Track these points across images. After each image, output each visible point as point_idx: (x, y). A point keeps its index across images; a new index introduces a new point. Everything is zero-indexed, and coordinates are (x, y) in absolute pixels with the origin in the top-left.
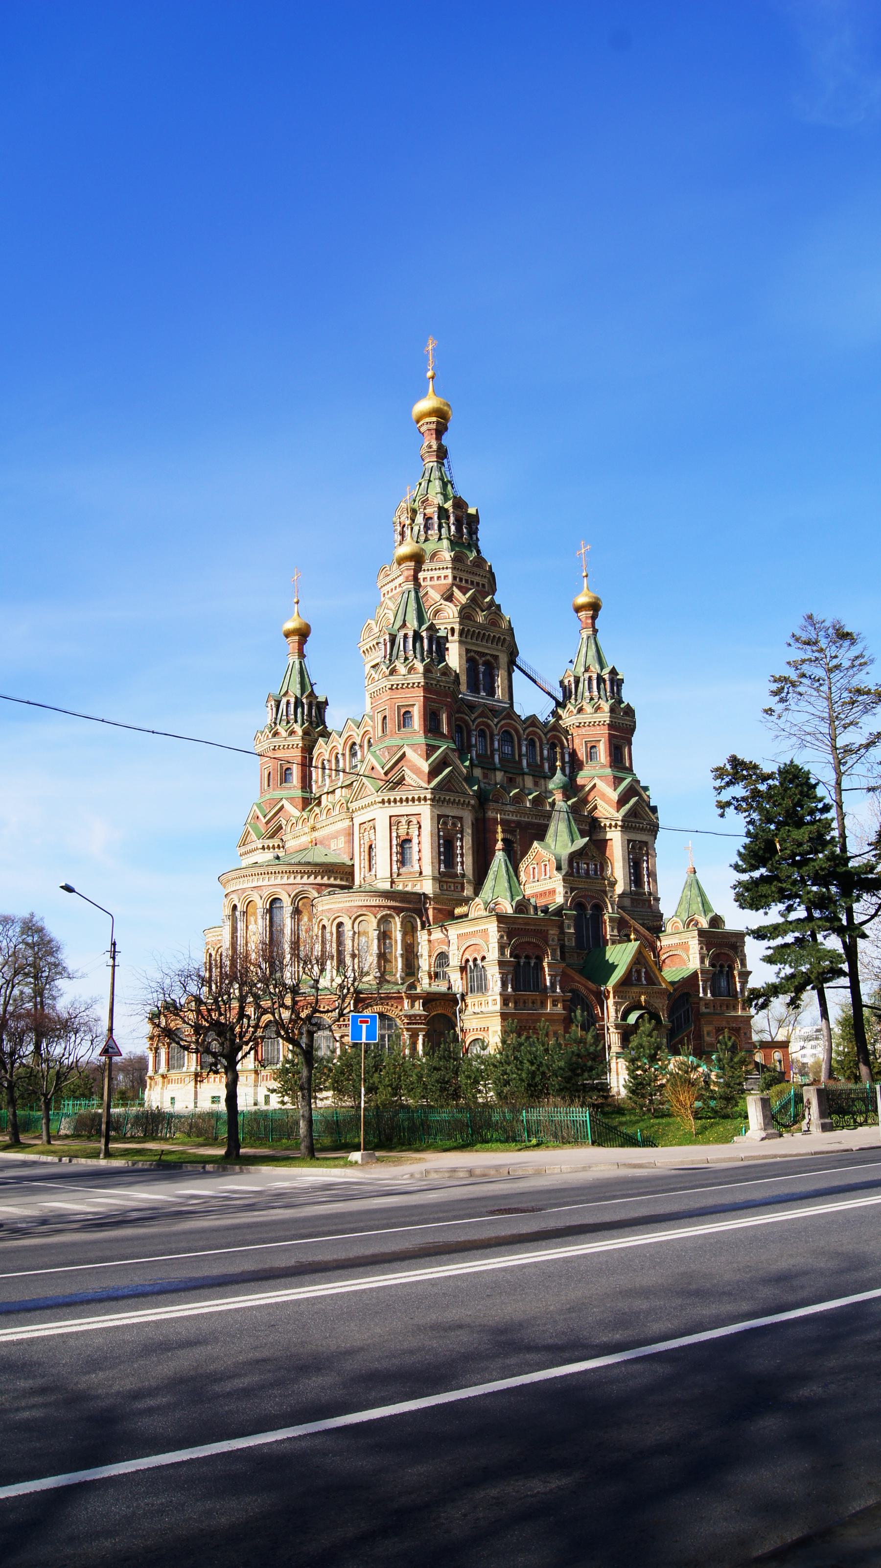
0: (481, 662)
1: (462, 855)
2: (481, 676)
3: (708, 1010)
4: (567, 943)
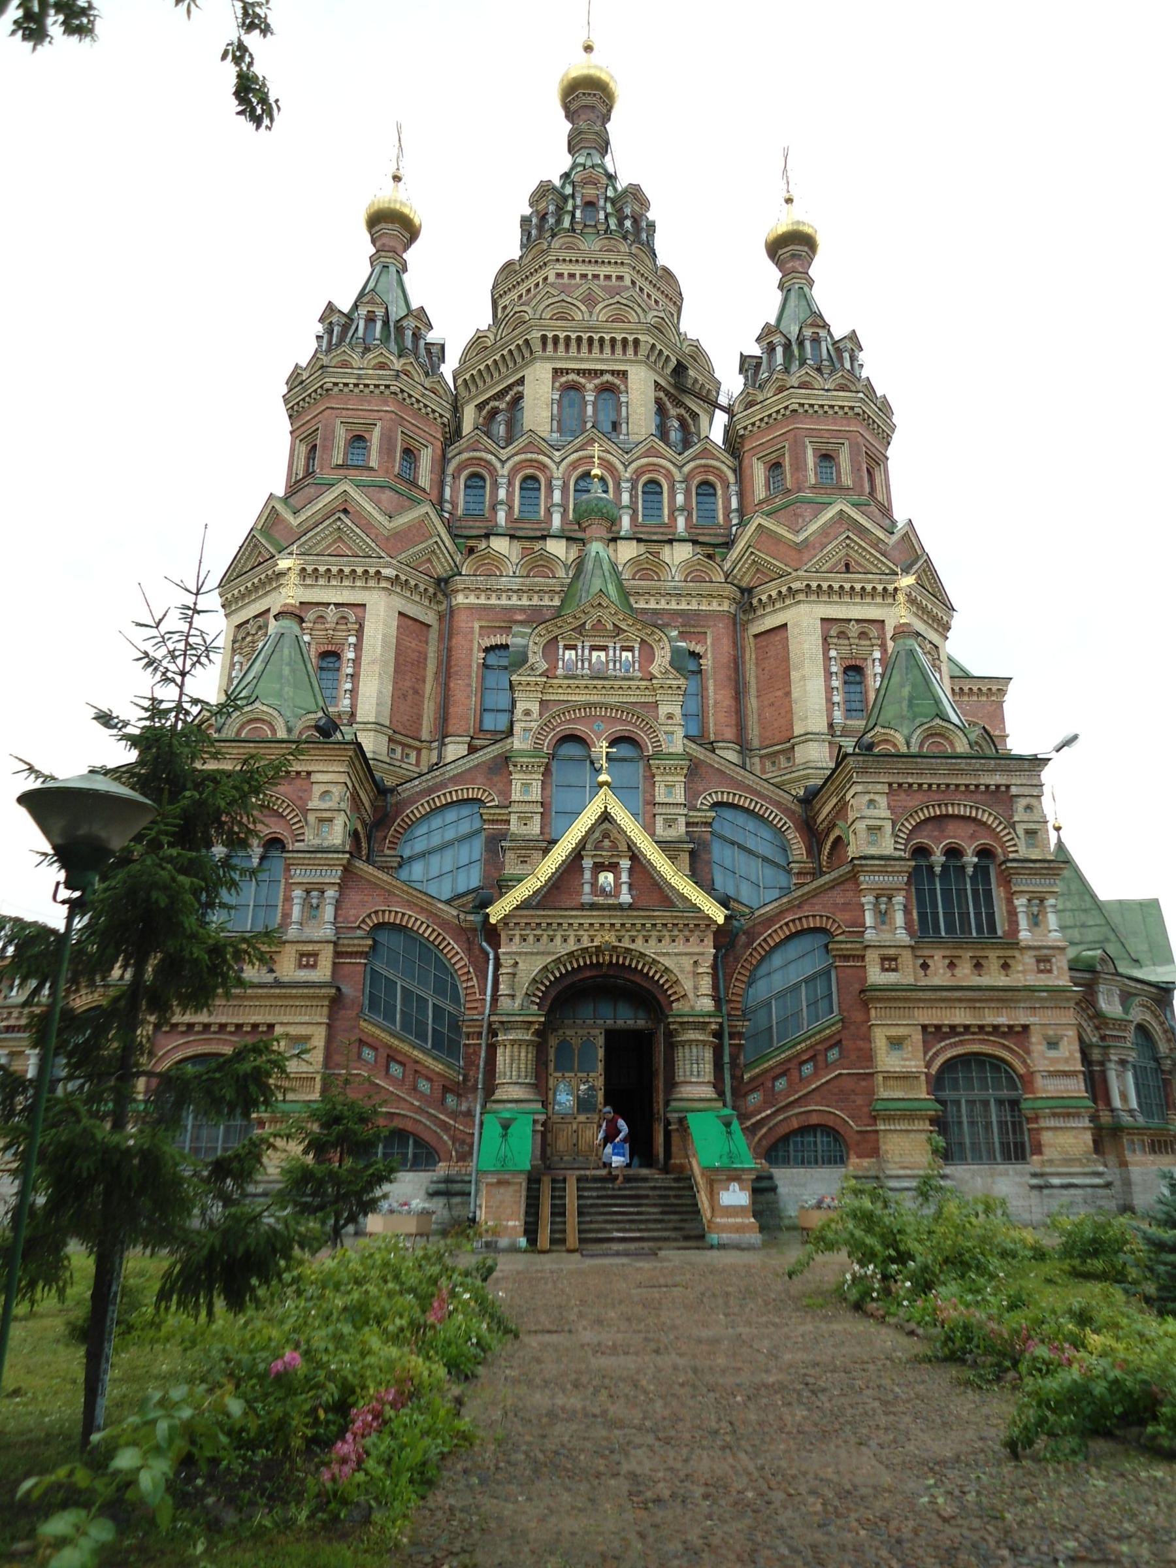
0: (590, 386)
1: (354, 677)
3: (891, 978)
4: (514, 827)
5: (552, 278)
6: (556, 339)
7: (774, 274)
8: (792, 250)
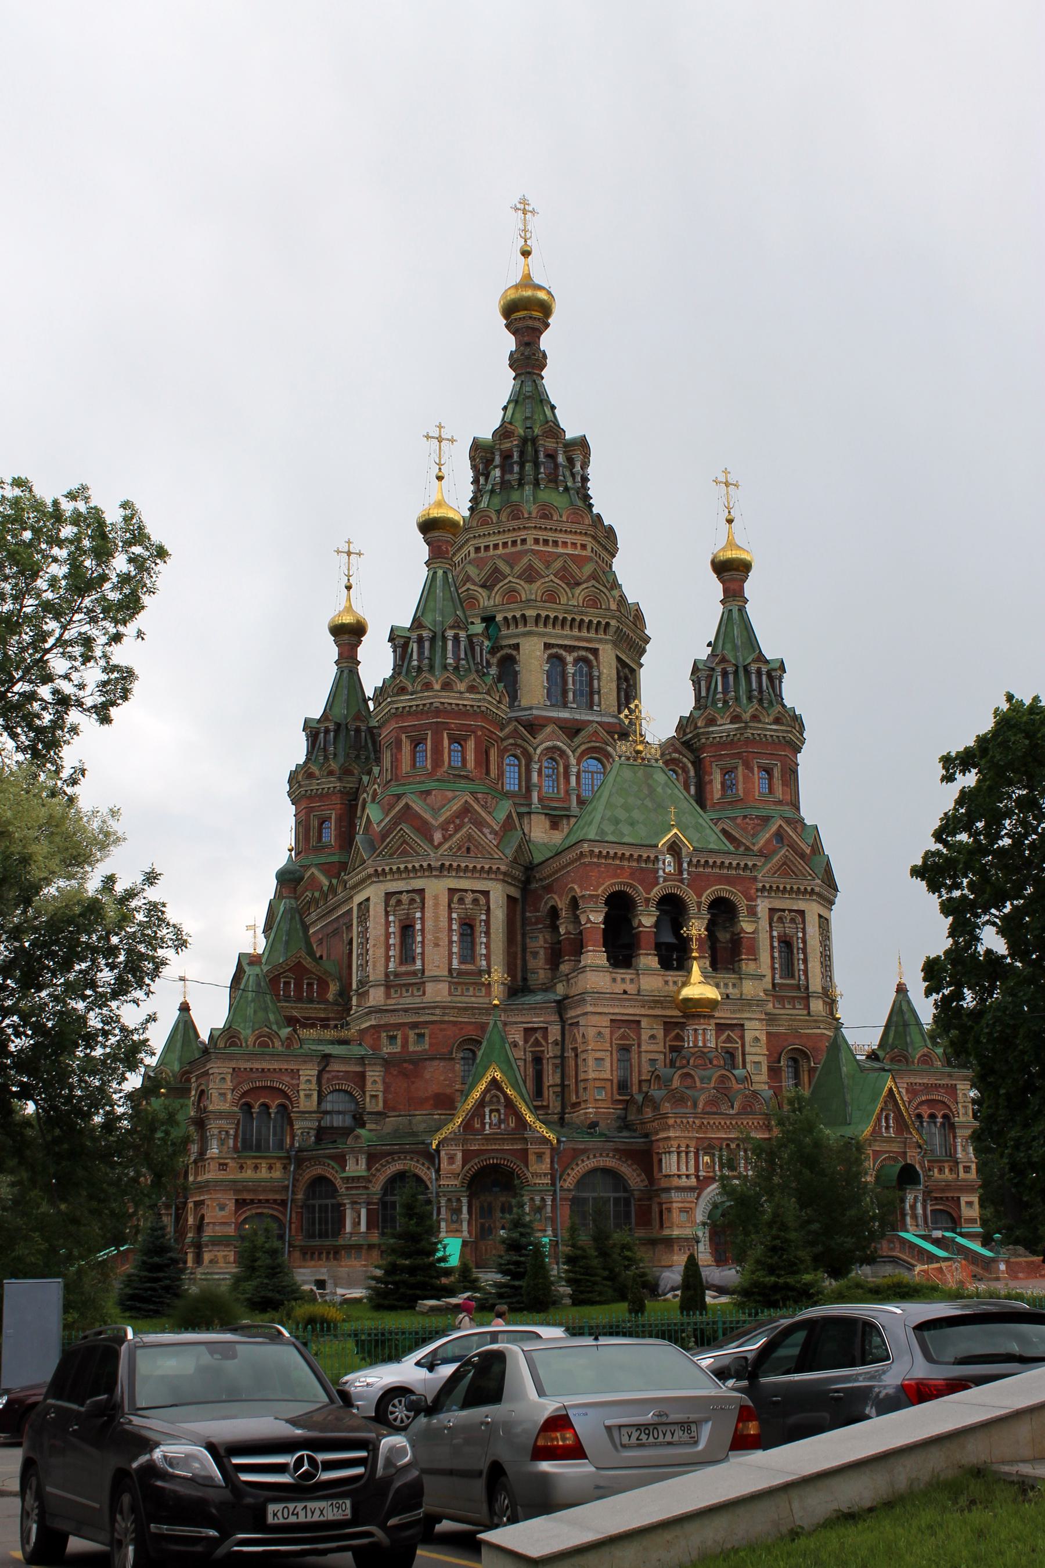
2: (570, 680)
5: (530, 541)
6: (547, 617)
7: (716, 588)
8: (731, 572)
